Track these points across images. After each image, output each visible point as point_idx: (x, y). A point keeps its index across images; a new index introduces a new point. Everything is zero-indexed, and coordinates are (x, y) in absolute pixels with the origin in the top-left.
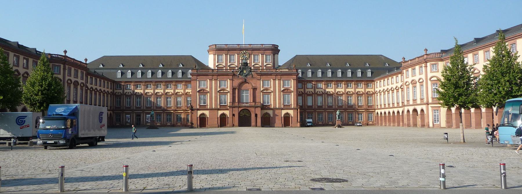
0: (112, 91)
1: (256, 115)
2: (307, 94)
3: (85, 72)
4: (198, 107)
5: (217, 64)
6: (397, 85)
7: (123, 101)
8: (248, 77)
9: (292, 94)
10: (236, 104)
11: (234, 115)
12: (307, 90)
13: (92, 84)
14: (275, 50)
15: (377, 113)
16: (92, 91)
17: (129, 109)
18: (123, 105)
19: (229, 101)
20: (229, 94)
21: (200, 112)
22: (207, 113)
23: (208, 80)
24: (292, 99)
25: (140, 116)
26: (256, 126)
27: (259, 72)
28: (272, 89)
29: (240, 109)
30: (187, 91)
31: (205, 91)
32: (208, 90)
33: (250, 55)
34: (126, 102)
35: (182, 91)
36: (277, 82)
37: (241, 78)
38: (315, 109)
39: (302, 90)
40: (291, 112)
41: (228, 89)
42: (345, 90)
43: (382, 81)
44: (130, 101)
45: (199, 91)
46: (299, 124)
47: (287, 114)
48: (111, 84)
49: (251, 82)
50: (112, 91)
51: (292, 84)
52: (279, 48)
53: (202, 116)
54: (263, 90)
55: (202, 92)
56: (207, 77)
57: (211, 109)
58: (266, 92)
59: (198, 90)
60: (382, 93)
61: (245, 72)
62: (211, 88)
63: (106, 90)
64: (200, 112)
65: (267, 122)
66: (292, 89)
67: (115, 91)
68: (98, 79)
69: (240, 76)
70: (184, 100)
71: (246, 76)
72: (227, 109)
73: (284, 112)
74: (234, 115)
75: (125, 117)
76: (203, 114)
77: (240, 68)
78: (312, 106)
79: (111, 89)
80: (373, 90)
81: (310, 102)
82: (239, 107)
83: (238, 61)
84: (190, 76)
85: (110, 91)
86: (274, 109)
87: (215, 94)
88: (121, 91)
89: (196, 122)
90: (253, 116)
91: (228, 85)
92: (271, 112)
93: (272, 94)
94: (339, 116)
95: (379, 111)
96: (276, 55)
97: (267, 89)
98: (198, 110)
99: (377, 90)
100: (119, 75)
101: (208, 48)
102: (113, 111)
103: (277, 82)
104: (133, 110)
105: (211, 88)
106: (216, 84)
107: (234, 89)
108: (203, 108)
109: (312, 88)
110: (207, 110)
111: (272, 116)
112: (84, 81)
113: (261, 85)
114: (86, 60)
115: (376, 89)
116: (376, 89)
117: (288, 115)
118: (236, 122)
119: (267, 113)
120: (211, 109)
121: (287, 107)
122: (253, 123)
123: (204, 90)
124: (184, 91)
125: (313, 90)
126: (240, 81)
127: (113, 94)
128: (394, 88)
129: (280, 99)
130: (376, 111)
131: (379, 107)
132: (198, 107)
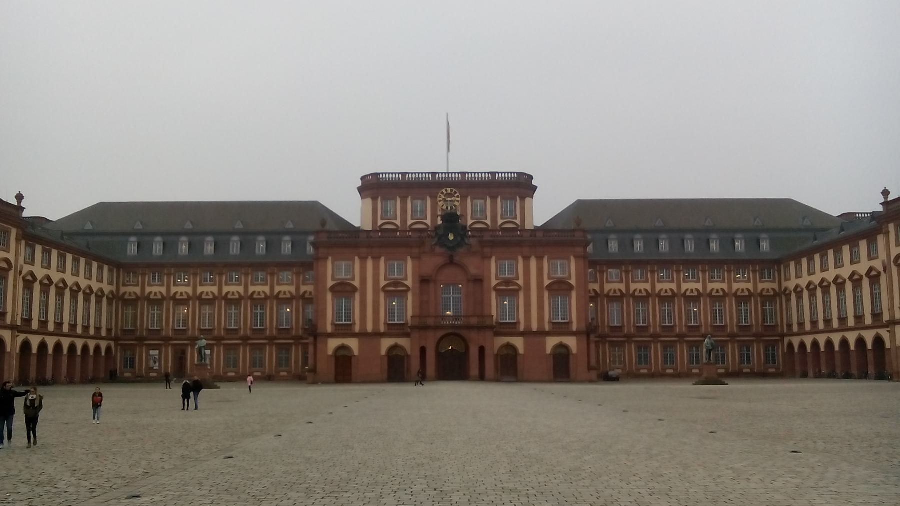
0: (114, 288)
1: (482, 350)
2: (608, 296)
3: (14, 231)
4: (329, 329)
5: (380, 222)
6: (825, 275)
7: (142, 314)
8: (461, 250)
9: (574, 294)
10: (431, 321)
11: (423, 350)
12: (608, 287)
13: (77, 274)
14: (522, 186)
15: (791, 345)
16: (90, 294)
17: (155, 333)
18: (142, 324)
19: (410, 313)
20: (410, 296)
22: (353, 344)
24: (573, 310)
25: (184, 352)
26: (482, 377)
27: (487, 237)
28: (521, 282)
29: (440, 333)
30: (303, 288)
32: (357, 283)
33: (464, 198)
34: (149, 319)
36: (533, 263)
38: (629, 336)
39: (596, 286)
40: (571, 342)
41: (409, 282)
42: (705, 287)
43: (817, 257)
44: (160, 316)
45: (332, 289)
46: (594, 374)
47: (561, 345)
48: (110, 270)
50: (114, 288)
51: (571, 269)
52: (534, 183)
53: (342, 352)
54: (498, 284)
55: (344, 290)
57: (362, 335)
58: (508, 289)
59: (330, 283)
60: (806, 294)
61: (451, 237)
63: (96, 286)
65: (509, 368)
66: (573, 281)
67: (123, 289)
68: (69, 257)
69: (438, 250)
71: (452, 249)
72: (407, 335)
73: (551, 342)
74: (423, 350)
75: (148, 354)
76: (343, 347)
77: (437, 228)
78: (620, 328)
79: (110, 283)
81: (614, 316)
82: (437, 328)
83: (434, 216)
84: (310, 250)
85: (107, 288)
86: (527, 333)
87: (375, 297)
88: (138, 290)
89: (326, 367)
90: (474, 352)
91: (408, 271)
92: (519, 342)
93: (522, 294)
94: (709, 351)
95: (796, 341)
96: (528, 200)
97: (508, 282)
98: (331, 335)
99: (791, 285)
100: (132, 249)
101: (360, 184)
102: (116, 339)
103: (533, 263)
104: (167, 339)
106: (376, 268)
108: (343, 330)
109: (621, 281)
110: (354, 335)
111: (521, 351)
112: (11, 256)
113: (494, 270)
114: (20, 197)
115: (785, 284)
116: (785, 284)
117: (563, 350)
118: (431, 369)
119: (510, 346)
120: (362, 335)
121: (561, 329)
122: (475, 371)
125: (622, 286)
126: (440, 260)
127: (116, 298)
128: (831, 280)
129: (541, 307)
130: (786, 340)
131: (795, 328)
132: (329, 329)
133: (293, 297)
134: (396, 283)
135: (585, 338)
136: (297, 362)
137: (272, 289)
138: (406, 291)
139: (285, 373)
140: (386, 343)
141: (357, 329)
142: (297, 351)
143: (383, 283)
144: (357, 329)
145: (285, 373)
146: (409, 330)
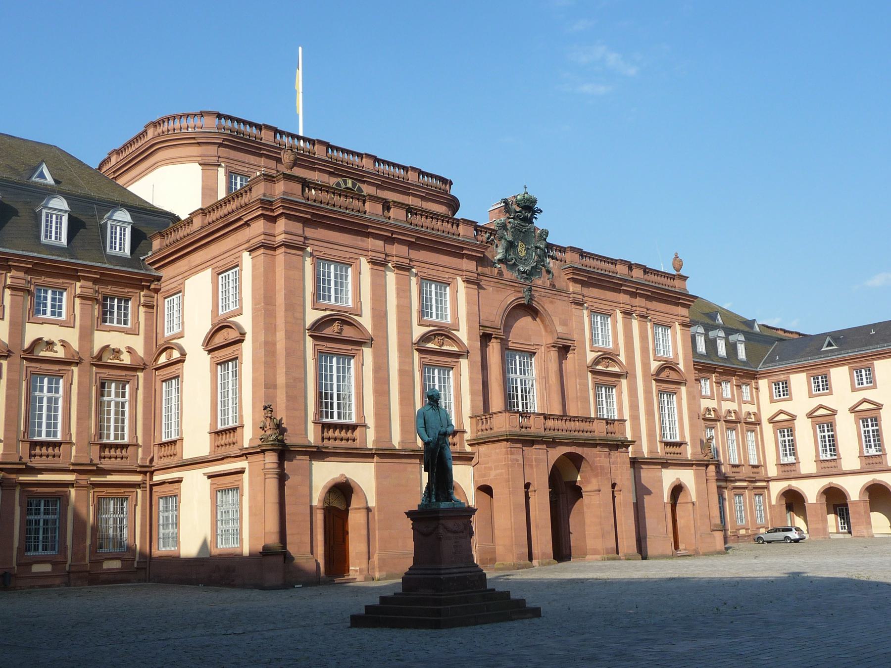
4: (312, 436)
8: (538, 281)
23: (365, 266)
31: (348, 333)
35: (72, 337)
37: (512, 284)
49: (549, 307)
56: (359, 241)
62: (380, 316)
64: (325, 473)
70: (83, 396)
71: (529, 275)
80: (753, 409)
98: (318, 454)
103: (635, 323)
105: (380, 316)
107: (486, 338)
110: (364, 455)
123: (345, 322)
124: (86, 336)
132: (312, 436)
139: (47, 568)
143: (418, 332)
145: (47, 568)
146: (468, 449)
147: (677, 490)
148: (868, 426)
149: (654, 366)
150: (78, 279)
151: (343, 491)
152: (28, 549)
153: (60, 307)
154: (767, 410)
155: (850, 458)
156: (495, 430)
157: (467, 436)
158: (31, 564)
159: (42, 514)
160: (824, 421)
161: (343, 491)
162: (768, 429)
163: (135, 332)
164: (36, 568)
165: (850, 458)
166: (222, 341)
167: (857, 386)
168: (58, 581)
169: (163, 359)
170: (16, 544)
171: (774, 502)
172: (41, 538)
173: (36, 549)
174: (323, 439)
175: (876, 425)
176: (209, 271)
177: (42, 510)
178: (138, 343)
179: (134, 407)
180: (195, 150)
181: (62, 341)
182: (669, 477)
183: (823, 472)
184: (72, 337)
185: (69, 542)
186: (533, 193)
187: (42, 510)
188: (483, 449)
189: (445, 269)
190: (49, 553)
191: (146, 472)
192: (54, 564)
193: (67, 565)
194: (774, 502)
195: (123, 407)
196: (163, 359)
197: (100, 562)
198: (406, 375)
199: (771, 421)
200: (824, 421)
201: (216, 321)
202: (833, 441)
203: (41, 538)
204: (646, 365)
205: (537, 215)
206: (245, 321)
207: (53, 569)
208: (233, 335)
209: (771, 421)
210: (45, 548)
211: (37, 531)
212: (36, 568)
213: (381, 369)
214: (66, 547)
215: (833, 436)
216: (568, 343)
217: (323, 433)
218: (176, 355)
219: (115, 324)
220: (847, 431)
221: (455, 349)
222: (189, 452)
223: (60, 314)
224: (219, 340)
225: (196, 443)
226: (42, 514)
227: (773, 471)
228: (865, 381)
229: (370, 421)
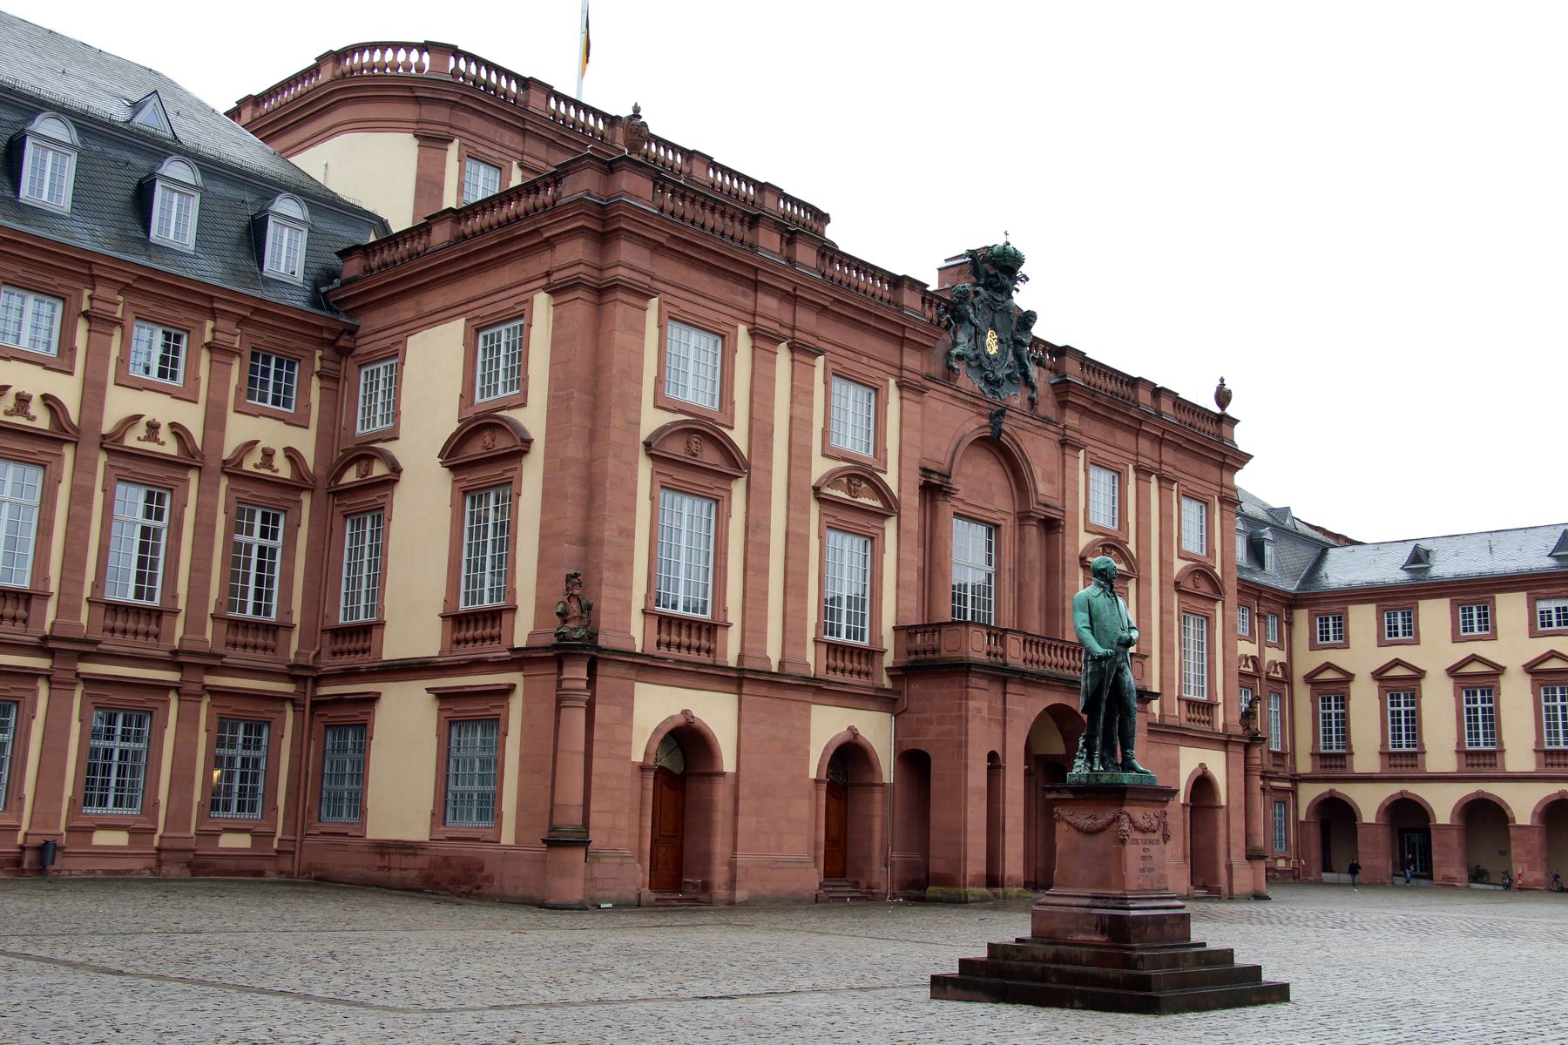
4: (638, 634)
21: (655, 706)
22: (716, 713)
54: (1091, 550)
59: (652, 420)
64: (655, 706)
98: (648, 667)
106: (801, 394)
132: (638, 634)
133: (189, 459)
134: (861, 475)
135: (1238, 755)
136: (181, 779)
137: (93, 394)
138: (882, 516)
139: (120, 839)
140: (828, 724)
141: (731, 649)
142: (187, 721)
144: (731, 649)
145: (120, 839)
147: (1203, 783)
148: (1475, 701)
149: (1179, 566)
150: (214, 314)
151: (687, 741)
152: (88, 801)
153: (175, 363)
154: (1306, 661)
155: (1440, 750)
156: (944, 653)
157: (888, 660)
158: (90, 831)
159: (118, 739)
160: (1400, 686)
161: (687, 741)
162: (1303, 694)
163: (300, 422)
164: (101, 838)
165: (1440, 750)
166: (482, 452)
167: (1540, 629)
168: (136, 864)
169: (351, 476)
170: (68, 791)
171: (1302, 817)
172: (113, 783)
173: (103, 802)
174: (659, 644)
175: (1490, 701)
176: (460, 323)
177: (119, 732)
178: (305, 442)
179: (289, 558)
180: (408, 111)
181: (173, 425)
182: (1190, 760)
183: (1392, 773)
184: (192, 417)
185: (163, 795)
186: (1017, 244)
187: (119, 732)
188: (916, 687)
189: (872, 363)
190: (124, 811)
191: (305, 678)
192: (134, 832)
193: (157, 837)
194: (1302, 817)
195: (273, 555)
196: (351, 476)
197: (216, 835)
198: (795, 540)
199: (1310, 679)
200: (1476, 684)
201: (469, 414)
202: (1413, 721)
203: (113, 783)
204: (1165, 564)
205: (1019, 285)
206: (533, 419)
207: (253, 842)
208: (503, 443)
209: (1310, 679)
210: (118, 802)
211: (107, 770)
212: (101, 838)
213: (756, 528)
214: (156, 804)
215: (1413, 713)
216: (1054, 514)
217: (659, 632)
218: (379, 470)
219: (269, 405)
220: (1439, 708)
221: (877, 504)
222: (394, 647)
223: (174, 376)
224: (475, 449)
225: (414, 630)
226: (118, 739)
227: (1304, 765)
228: (1476, 626)
229: (734, 616)
